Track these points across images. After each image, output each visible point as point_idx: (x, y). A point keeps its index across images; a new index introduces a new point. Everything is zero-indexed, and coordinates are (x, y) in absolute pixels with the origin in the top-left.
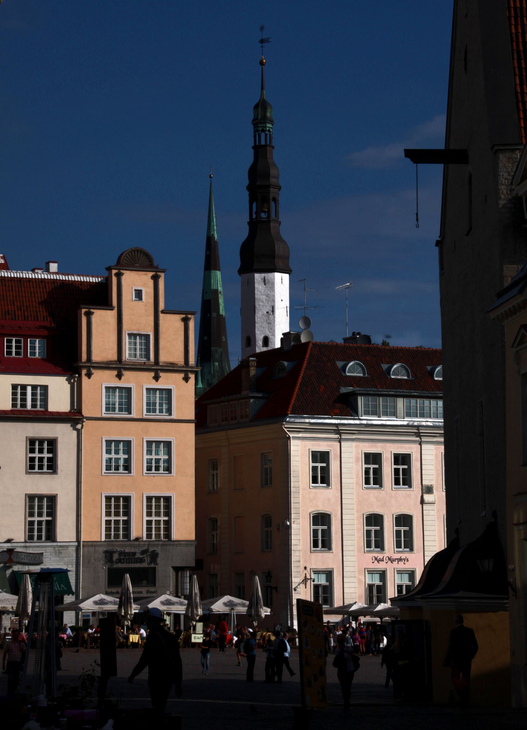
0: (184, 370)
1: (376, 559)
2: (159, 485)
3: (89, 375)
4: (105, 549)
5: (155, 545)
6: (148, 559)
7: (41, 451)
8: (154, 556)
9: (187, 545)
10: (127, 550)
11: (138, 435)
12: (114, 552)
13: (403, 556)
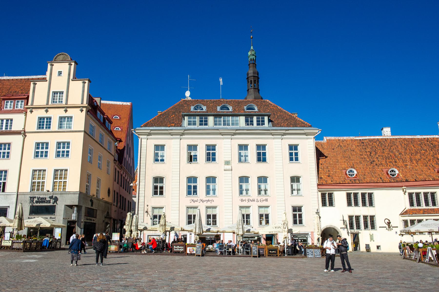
0: (81, 108)
1: (193, 200)
2: (61, 164)
3: (31, 112)
4: (30, 196)
5: (56, 194)
6: (52, 201)
7: (5, 149)
8: (56, 200)
9: (74, 194)
10: (41, 196)
11: (52, 139)
12: (35, 198)
13: (210, 199)
